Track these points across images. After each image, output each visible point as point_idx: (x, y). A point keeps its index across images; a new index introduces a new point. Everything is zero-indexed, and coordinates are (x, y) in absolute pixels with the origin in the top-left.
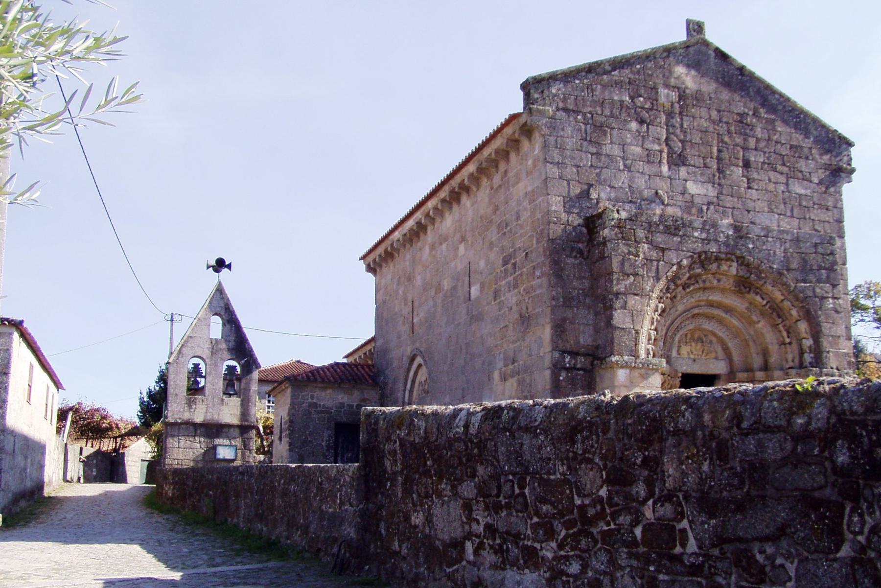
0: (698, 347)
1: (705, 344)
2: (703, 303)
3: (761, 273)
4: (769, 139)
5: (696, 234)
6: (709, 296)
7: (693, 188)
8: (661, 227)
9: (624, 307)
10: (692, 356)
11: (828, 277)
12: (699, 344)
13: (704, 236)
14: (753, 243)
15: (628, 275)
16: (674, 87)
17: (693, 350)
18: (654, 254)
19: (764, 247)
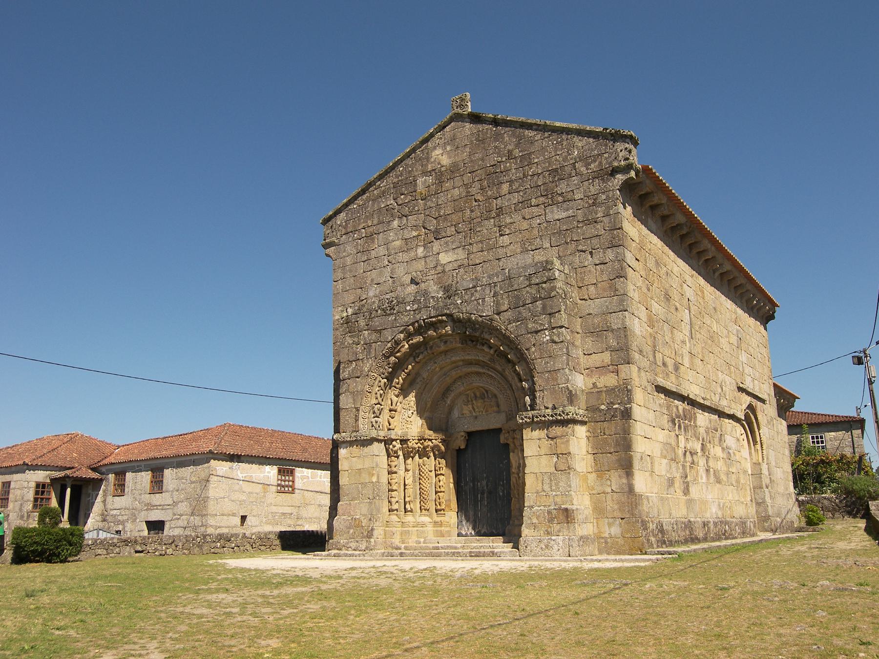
0: (479, 404)
1: (486, 400)
2: (461, 363)
3: (474, 325)
4: (525, 176)
5: (408, 308)
6: (452, 357)
7: (444, 258)
8: (379, 311)
9: (347, 390)
10: (474, 414)
11: (544, 307)
12: (481, 401)
13: (416, 306)
14: (461, 298)
15: (351, 362)
16: (430, 172)
17: (475, 407)
18: (374, 336)
19: (473, 298)
